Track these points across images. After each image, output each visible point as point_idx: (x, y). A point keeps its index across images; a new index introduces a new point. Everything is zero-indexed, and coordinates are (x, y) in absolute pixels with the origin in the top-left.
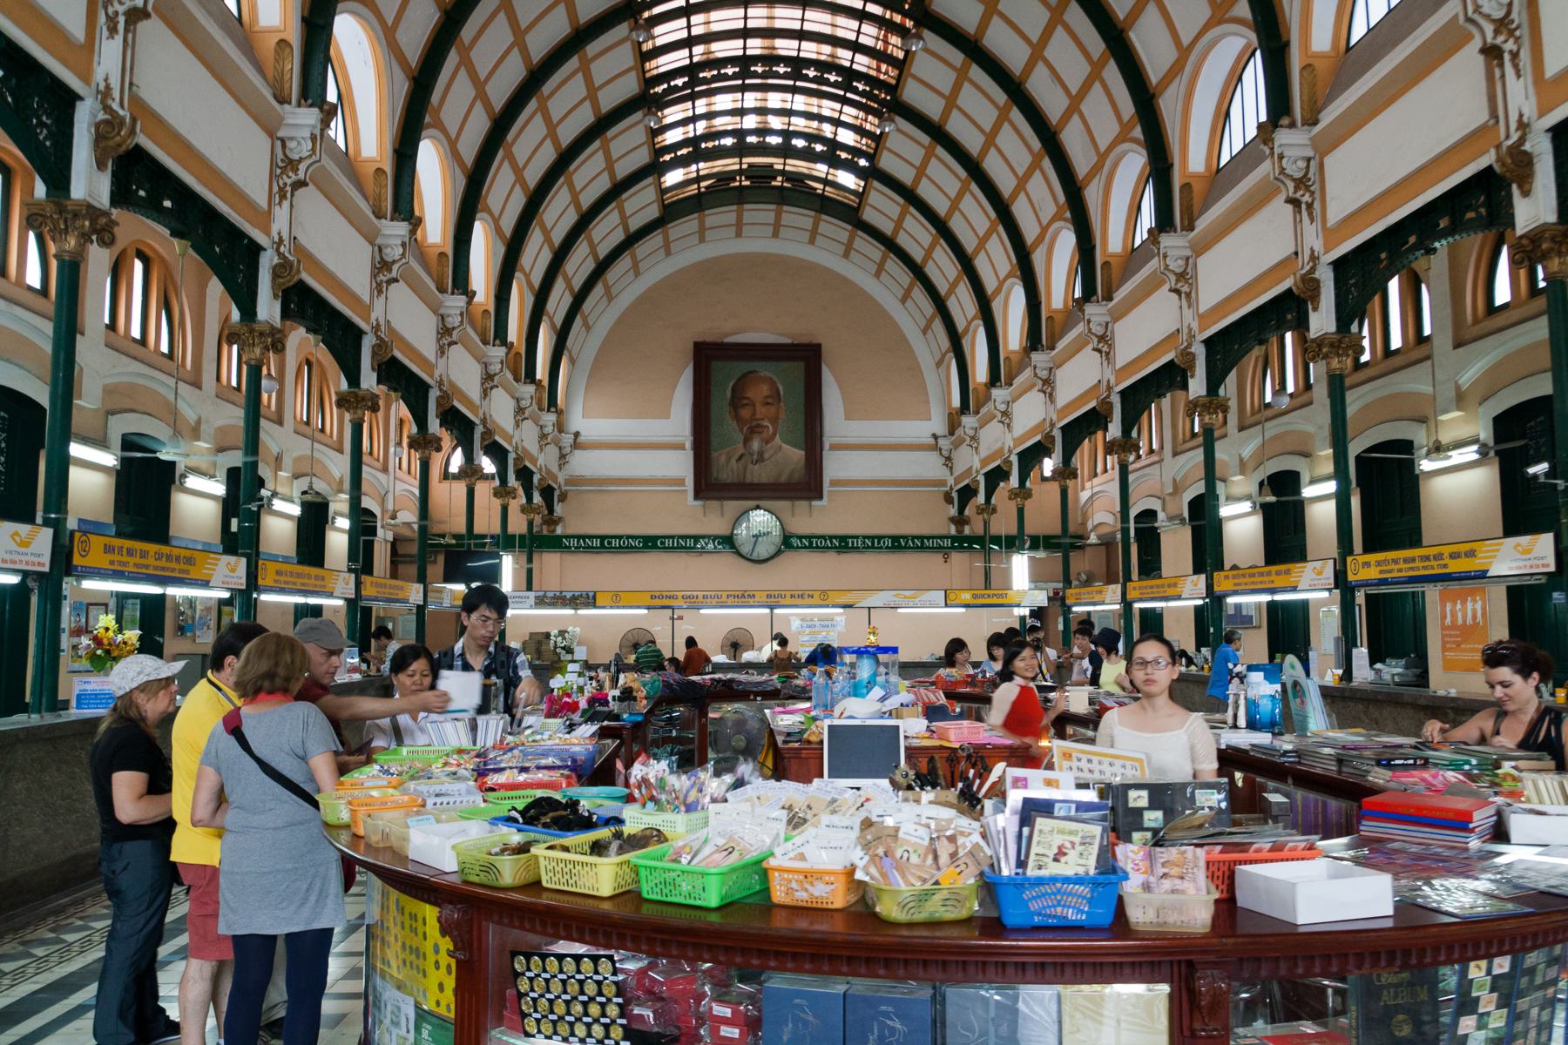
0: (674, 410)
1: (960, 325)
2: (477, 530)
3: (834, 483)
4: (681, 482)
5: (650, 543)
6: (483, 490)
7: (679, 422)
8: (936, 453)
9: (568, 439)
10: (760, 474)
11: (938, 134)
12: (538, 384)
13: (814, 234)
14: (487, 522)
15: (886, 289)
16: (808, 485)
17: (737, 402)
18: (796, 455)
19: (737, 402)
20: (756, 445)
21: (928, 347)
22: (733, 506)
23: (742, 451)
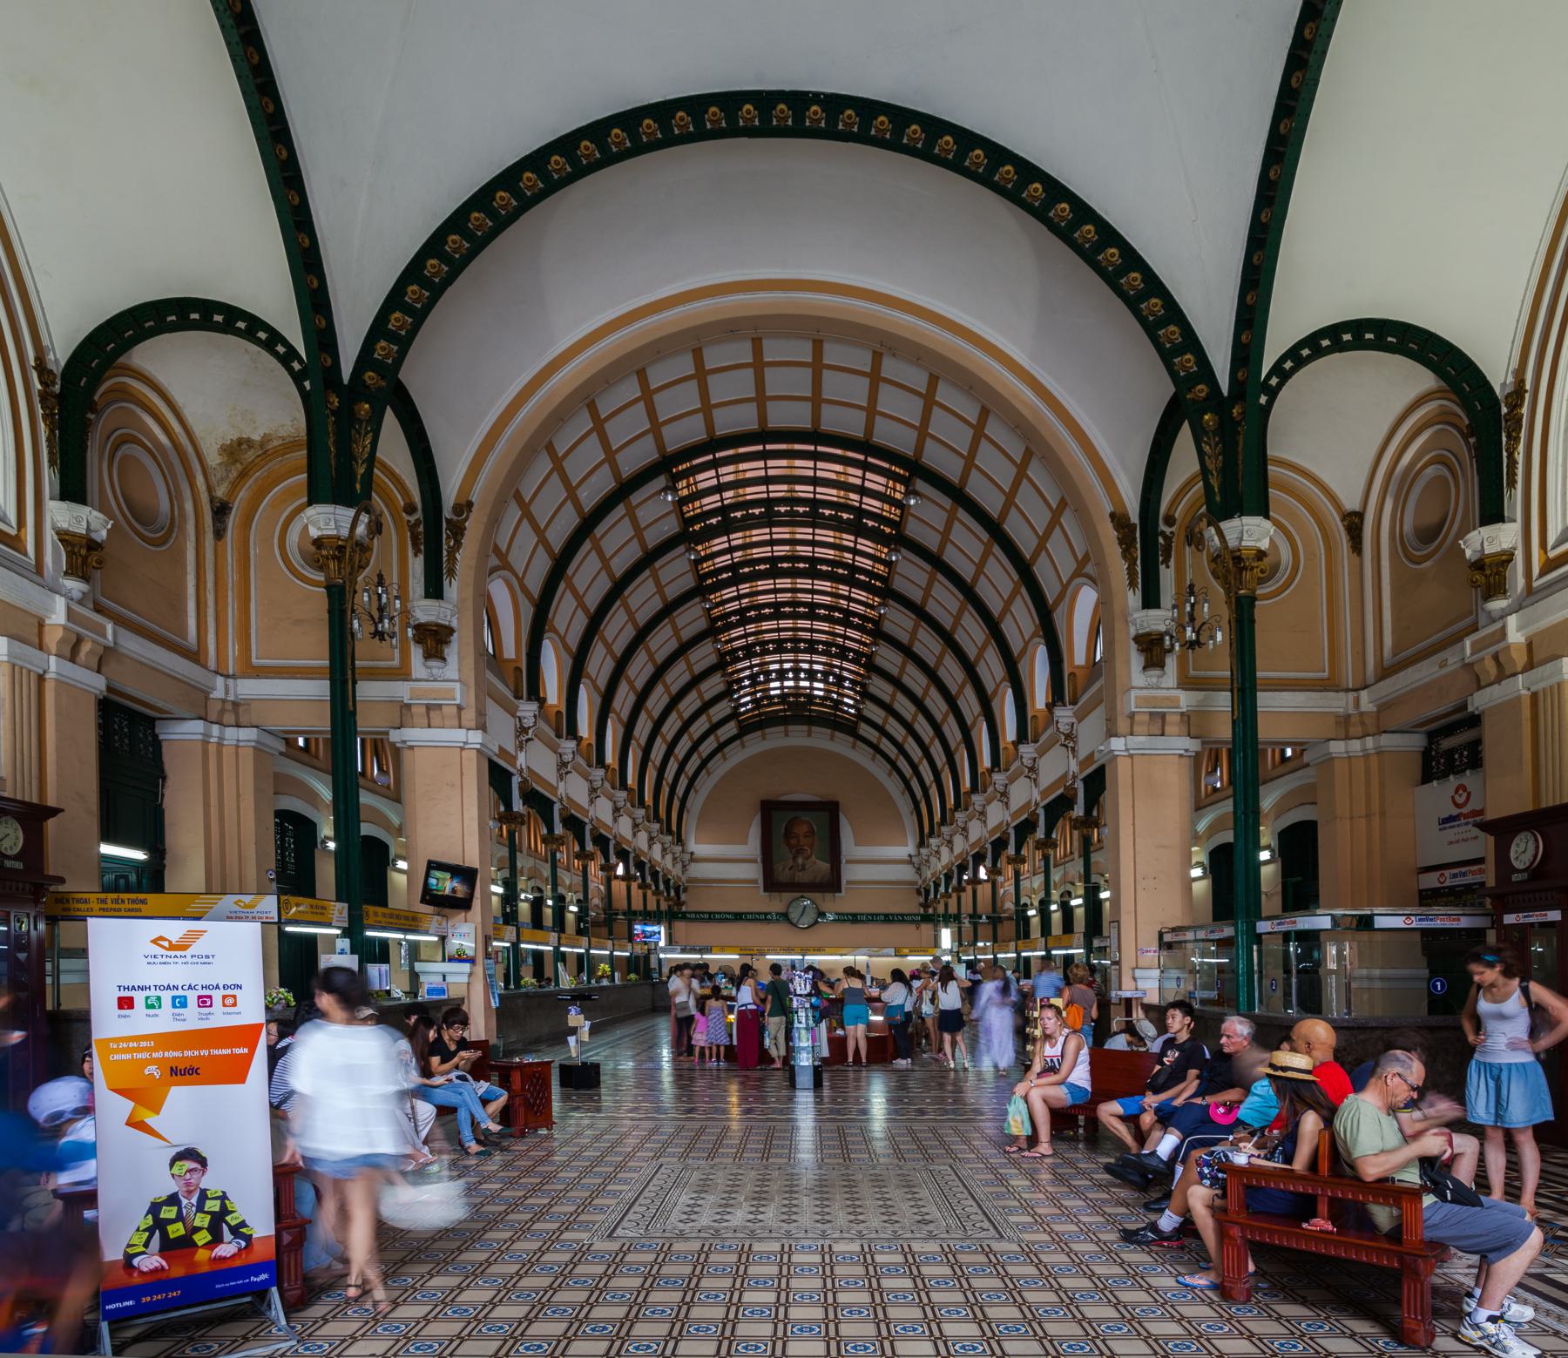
0: (751, 839)
1: (953, 746)
2: (634, 907)
3: (848, 882)
4: (755, 881)
5: (738, 917)
6: (634, 885)
7: (753, 847)
8: (910, 867)
9: (687, 857)
10: (803, 877)
11: (958, 495)
12: (647, 808)
13: (832, 738)
14: (652, 906)
15: (879, 770)
16: (832, 884)
17: (788, 834)
18: (825, 866)
19: (788, 834)
20: (800, 861)
21: (904, 805)
22: (787, 896)
23: (791, 863)
